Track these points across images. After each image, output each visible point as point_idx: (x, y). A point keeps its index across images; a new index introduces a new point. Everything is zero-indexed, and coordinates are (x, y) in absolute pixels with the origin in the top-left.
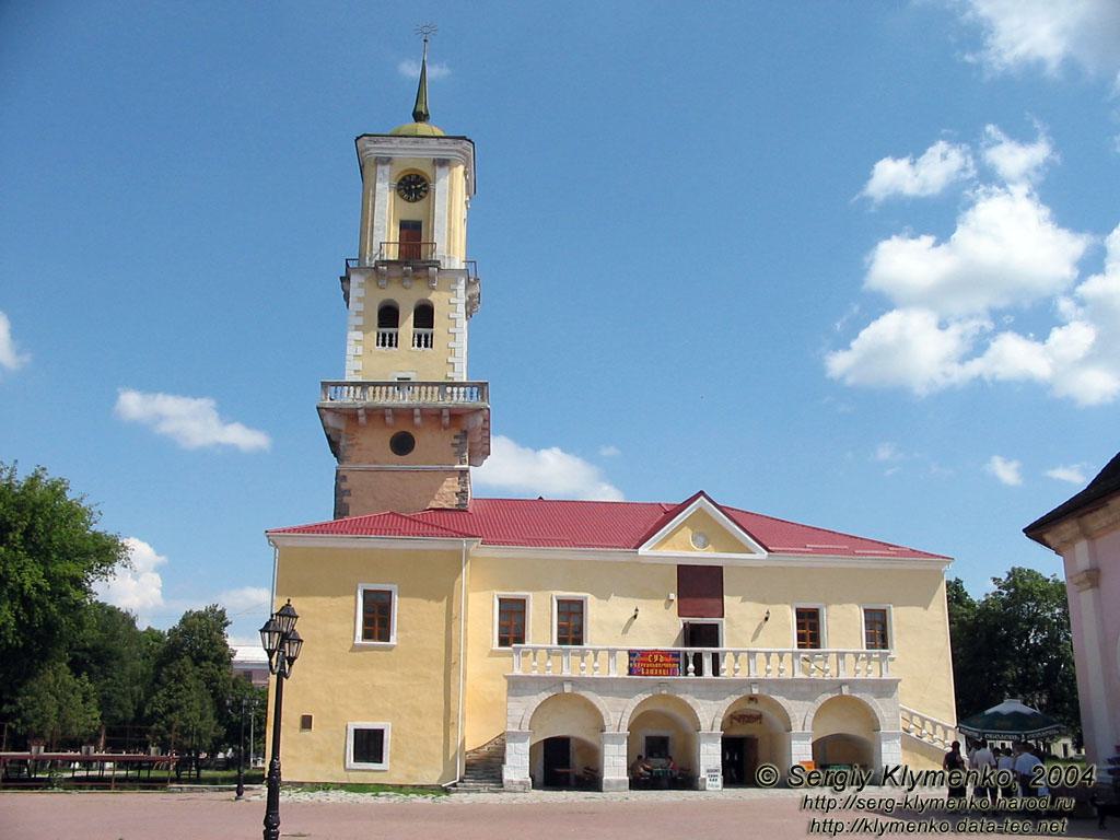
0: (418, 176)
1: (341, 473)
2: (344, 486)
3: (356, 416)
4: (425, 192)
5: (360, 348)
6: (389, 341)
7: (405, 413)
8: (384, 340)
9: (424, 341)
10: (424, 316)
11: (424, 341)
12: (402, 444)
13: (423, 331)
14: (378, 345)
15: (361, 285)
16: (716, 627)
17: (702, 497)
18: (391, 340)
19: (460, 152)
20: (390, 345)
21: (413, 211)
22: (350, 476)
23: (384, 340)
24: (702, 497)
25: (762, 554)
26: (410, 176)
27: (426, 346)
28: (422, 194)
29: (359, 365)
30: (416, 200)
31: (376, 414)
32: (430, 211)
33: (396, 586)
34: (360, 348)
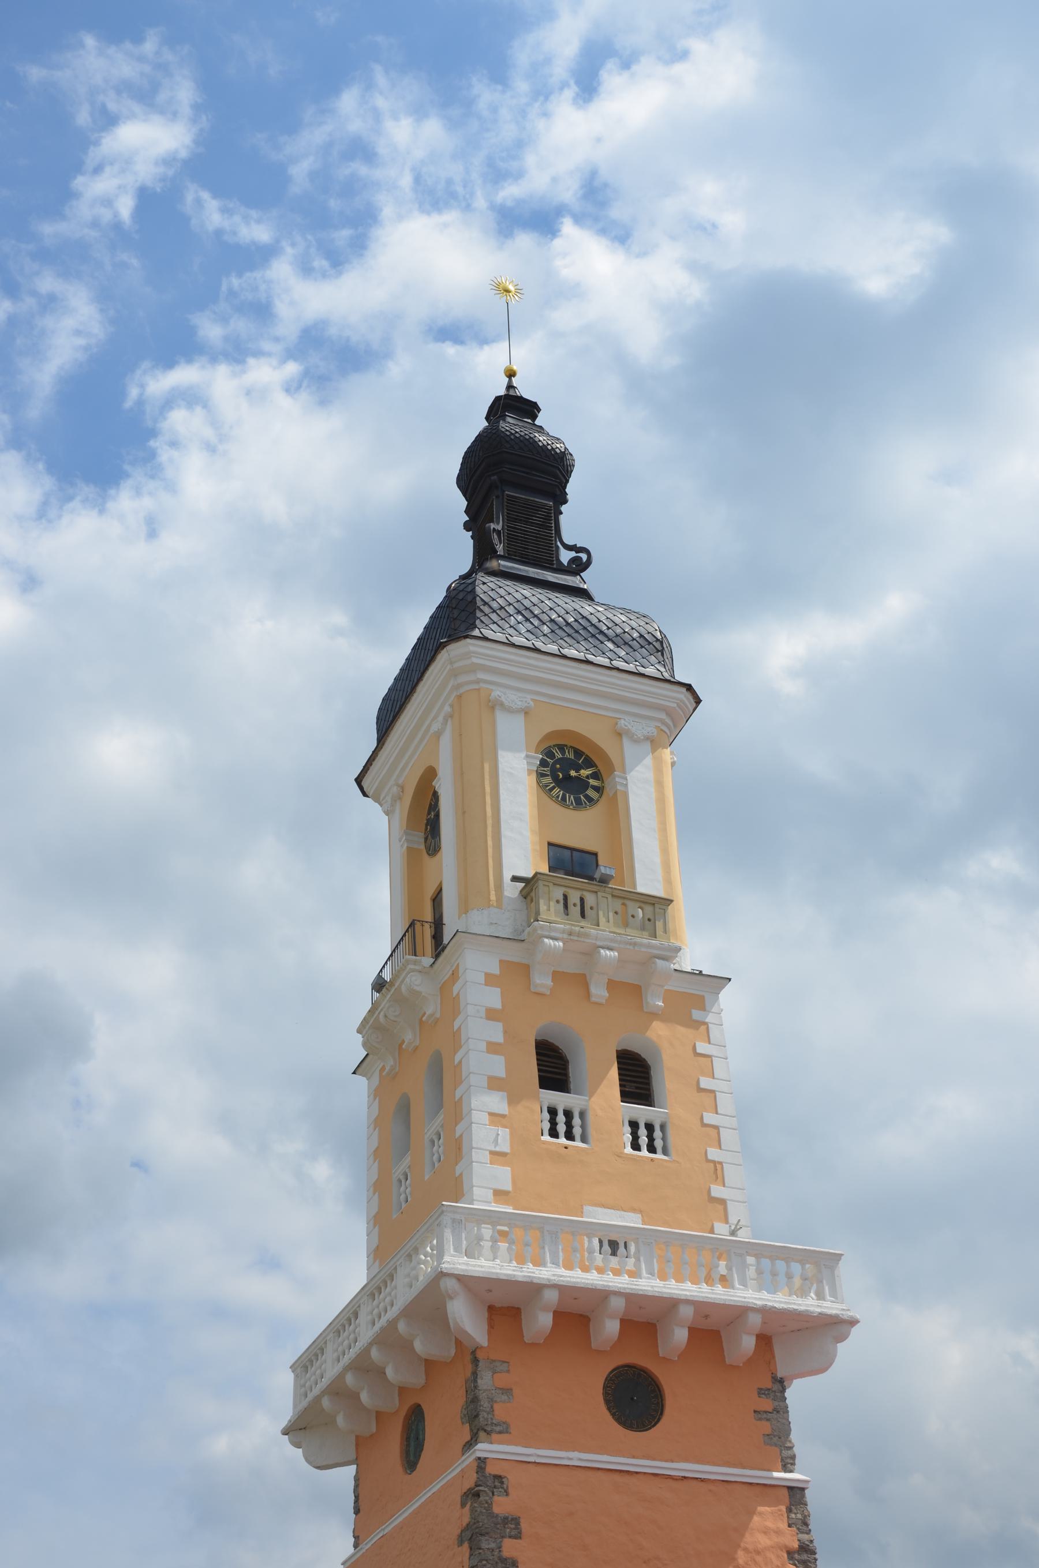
0: (578, 753)
1: (490, 1470)
2: (502, 1506)
4: (597, 789)
5: (504, 1133)
7: (645, 1320)
8: (553, 1123)
13: (641, 1112)
19: (668, 712)
20: (569, 1136)
21: (580, 829)
22: (513, 1478)
23: (553, 1123)
26: (562, 748)
27: (652, 1149)
28: (590, 792)
29: (503, 1177)
34: (504, 1133)
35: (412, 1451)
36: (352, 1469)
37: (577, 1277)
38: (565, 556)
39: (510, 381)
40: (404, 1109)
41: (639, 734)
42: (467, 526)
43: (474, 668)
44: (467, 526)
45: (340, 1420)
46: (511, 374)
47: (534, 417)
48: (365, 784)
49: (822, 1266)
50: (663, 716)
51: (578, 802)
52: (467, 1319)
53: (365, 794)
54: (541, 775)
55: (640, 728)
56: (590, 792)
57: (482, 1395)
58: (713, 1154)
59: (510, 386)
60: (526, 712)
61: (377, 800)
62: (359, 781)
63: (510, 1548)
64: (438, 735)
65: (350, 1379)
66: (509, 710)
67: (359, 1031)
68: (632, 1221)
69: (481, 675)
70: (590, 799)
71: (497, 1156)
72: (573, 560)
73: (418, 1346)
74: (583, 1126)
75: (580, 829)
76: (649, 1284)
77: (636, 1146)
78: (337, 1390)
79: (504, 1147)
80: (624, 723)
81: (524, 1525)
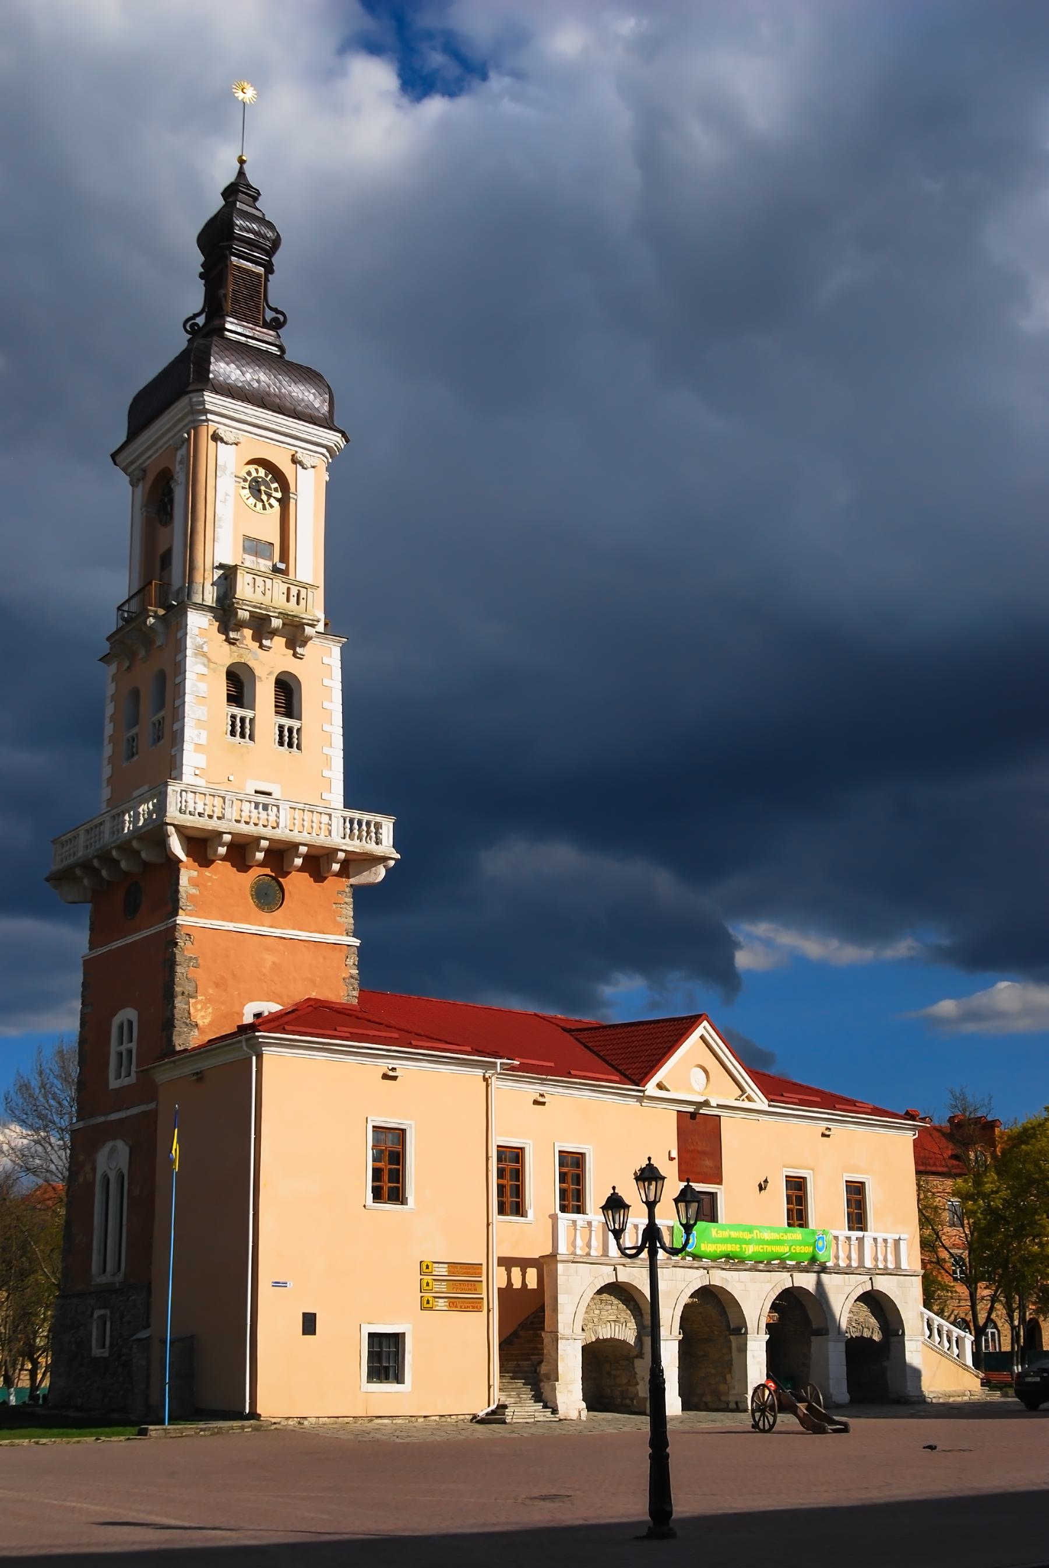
6: (241, 729)
8: (233, 725)
9: (288, 739)
11: (288, 739)
12: (269, 897)
13: (287, 722)
16: (713, 1196)
17: (705, 1023)
20: (243, 736)
22: (195, 934)
24: (705, 1023)
25: (761, 1103)
27: (290, 745)
31: (240, 852)
33: (412, 1123)
34: (204, 733)
35: (132, 907)
36: (90, 905)
37: (243, 829)
38: (269, 315)
39: (241, 168)
40: (135, 695)
41: (308, 464)
42: (202, 276)
43: (206, 412)
44: (202, 276)
45: (86, 882)
46: (242, 162)
47: (255, 199)
48: (118, 460)
50: (324, 451)
51: (264, 508)
52: (176, 846)
53: (115, 464)
57: (181, 889)
58: (326, 750)
59: (241, 173)
60: (236, 444)
61: (124, 470)
62: (113, 456)
63: (192, 972)
64: (177, 449)
65: (96, 863)
66: (226, 443)
67: (108, 639)
69: (210, 416)
70: (271, 506)
71: (198, 747)
72: (275, 319)
73: (144, 855)
76: (282, 833)
77: (281, 744)
78: (86, 866)
79: (203, 741)
80: (299, 456)
81: (200, 961)
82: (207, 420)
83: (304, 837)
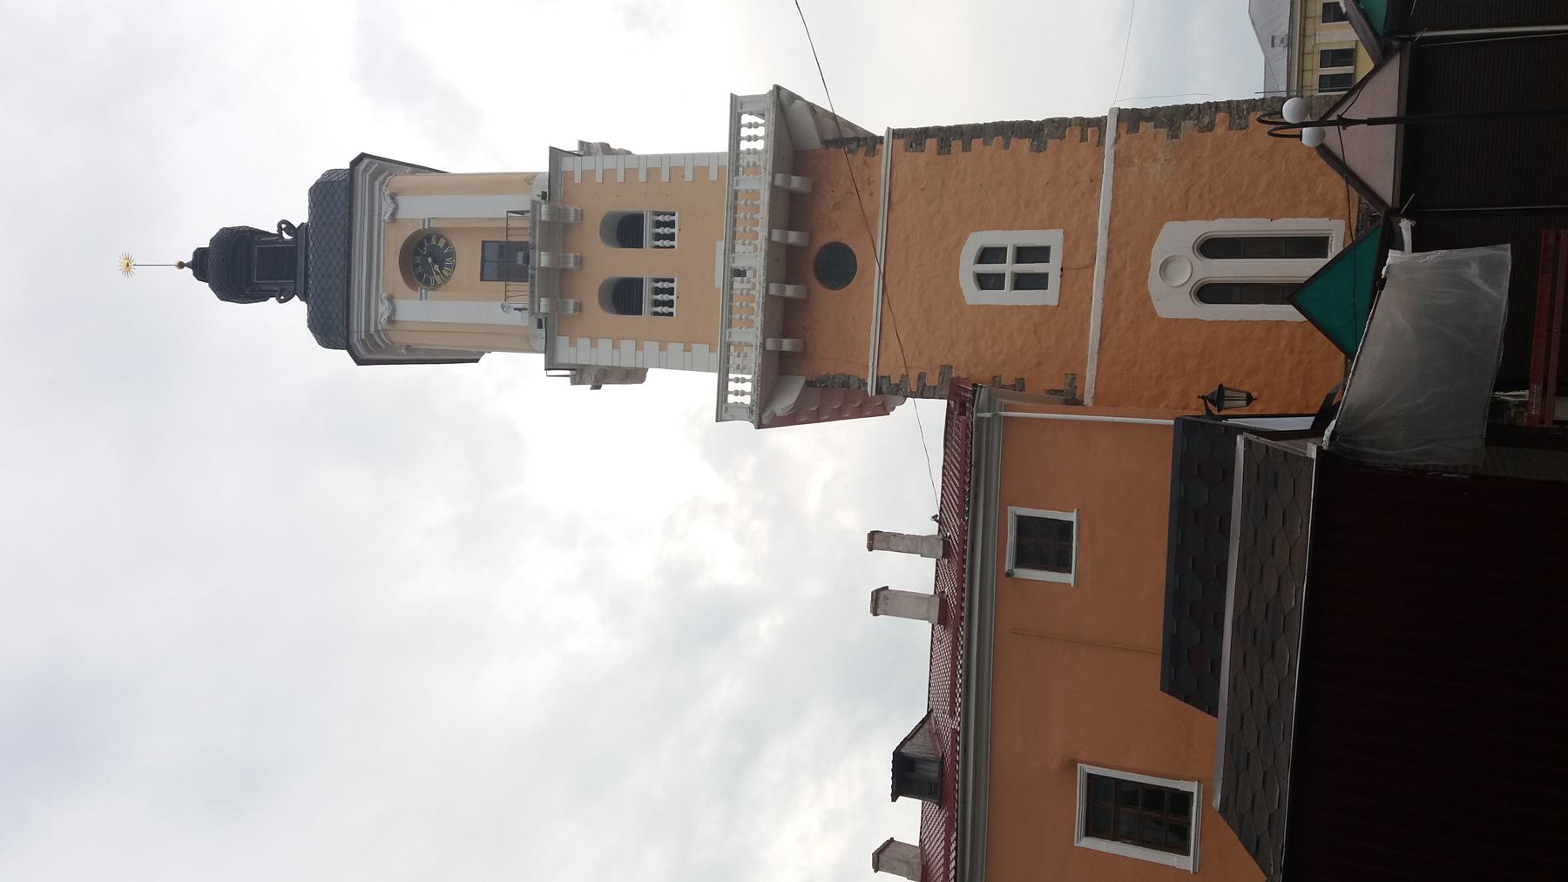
3: (783, 356)
4: (439, 238)
8: (663, 303)
10: (627, 230)
14: (671, 314)
15: (573, 344)
18: (664, 291)
21: (468, 259)
23: (663, 303)
28: (441, 244)
30: (452, 254)
32: (466, 229)
49: (738, 106)
50: (377, 183)
54: (436, 286)
55: (387, 207)
56: (441, 244)
60: (391, 299)
66: (394, 310)
68: (720, 246)
74: (664, 280)
75: (468, 259)
80: (386, 217)
82: (377, 331)
83: (762, 232)
